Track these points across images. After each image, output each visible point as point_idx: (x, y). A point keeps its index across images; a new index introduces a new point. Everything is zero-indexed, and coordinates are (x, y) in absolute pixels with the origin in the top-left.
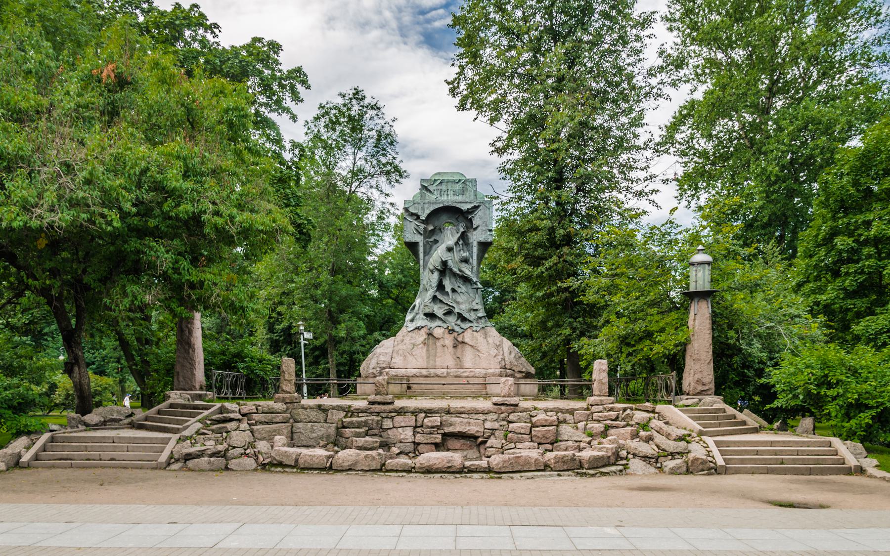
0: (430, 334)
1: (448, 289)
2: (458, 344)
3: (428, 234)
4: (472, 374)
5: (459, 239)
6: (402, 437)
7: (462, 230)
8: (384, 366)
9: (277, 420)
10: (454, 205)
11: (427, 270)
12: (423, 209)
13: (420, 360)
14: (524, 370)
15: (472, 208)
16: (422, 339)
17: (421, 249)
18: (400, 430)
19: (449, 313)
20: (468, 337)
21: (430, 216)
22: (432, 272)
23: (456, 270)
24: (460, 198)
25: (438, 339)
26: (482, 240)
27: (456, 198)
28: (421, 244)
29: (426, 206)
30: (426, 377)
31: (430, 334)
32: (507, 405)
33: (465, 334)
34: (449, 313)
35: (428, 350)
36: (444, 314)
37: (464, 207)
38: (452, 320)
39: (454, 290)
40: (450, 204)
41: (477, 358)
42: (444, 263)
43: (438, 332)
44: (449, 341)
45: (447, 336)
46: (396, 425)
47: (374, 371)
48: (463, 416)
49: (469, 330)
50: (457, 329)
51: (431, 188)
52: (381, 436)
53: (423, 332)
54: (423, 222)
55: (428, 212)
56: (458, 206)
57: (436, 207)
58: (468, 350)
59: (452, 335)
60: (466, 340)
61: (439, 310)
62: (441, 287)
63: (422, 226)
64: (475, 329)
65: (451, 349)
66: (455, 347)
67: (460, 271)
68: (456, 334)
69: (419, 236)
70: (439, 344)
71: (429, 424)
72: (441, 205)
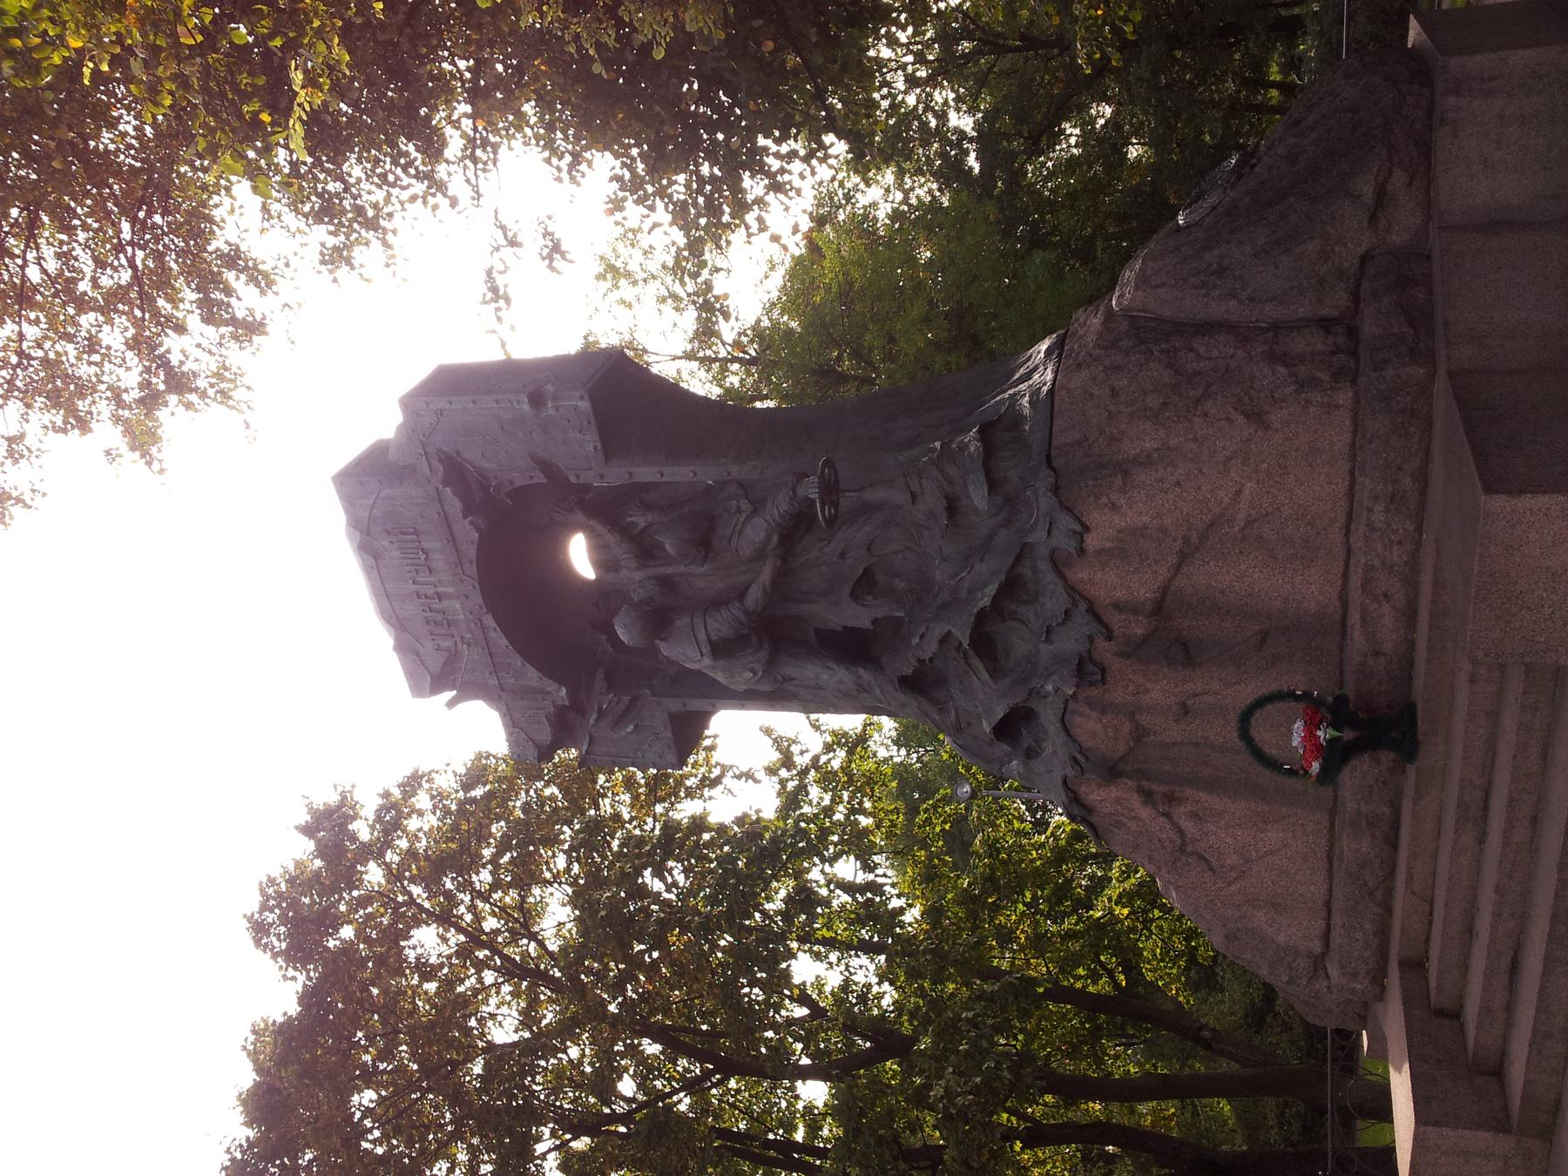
1: (860, 616)
10: (472, 570)
13: (1274, 836)
25: (1139, 734)
26: (590, 442)
28: (675, 705)
35: (1213, 786)
36: (995, 672)
38: (1019, 641)
45: (1118, 696)
49: (1080, 574)
50: (1069, 642)
56: (471, 551)
59: (1115, 664)
60: (1144, 589)
64: (1066, 544)
67: (759, 556)
72: (489, 621)
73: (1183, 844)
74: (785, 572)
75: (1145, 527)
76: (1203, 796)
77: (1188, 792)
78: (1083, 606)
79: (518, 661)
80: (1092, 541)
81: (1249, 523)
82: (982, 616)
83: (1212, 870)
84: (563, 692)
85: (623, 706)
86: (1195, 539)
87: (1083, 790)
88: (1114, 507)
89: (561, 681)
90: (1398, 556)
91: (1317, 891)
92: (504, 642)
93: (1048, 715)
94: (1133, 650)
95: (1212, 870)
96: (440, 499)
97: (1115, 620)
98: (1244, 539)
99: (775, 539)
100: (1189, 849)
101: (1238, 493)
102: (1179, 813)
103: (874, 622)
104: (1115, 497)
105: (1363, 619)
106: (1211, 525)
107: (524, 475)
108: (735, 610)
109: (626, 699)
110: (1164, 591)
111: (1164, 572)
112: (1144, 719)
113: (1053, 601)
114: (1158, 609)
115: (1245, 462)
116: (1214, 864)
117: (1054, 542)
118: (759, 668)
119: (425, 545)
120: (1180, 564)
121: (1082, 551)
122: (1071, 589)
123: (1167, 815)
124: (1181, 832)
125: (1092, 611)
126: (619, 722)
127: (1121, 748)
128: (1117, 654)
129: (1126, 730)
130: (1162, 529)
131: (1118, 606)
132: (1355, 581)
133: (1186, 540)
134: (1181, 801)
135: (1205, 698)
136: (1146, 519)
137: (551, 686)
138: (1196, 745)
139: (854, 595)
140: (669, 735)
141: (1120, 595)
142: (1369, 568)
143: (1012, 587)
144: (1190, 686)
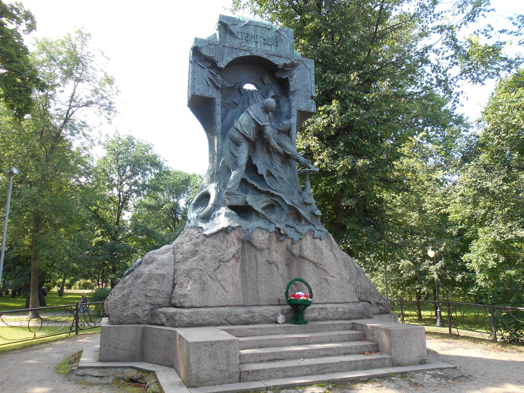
0: (247, 242)
1: (262, 170)
3: (225, 91)
4: (324, 313)
8: (160, 300)
10: (265, 56)
11: (228, 140)
13: (230, 289)
16: (233, 250)
17: (218, 109)
19: (270, 207)
21: (231, 64)
22: (237, 144)
23: (273, 143)
24: (272, 49)
25: (261, 250)
26: (303, 108)
27: (268, 48)
28: (218, 101)
29: (227, 50)
30: (247, 323)
31: (247, 242)
33: (304, 242)
34: (270, 207)
36: (264, 209)
37: (279, 62)
39: (269, 174)
41: (324, 284)
42: (260, 130)
43: (260, 238)
44: (278, 255)
45: (274, 245)
47: (139, 311)
50: (291, 233)
51: (232, 28)
53: (233, 237)
55: (230, 59)
56: (271, 59)
57: (241, 54)
59: (284, 244)
60: (308, 253)
61: (258, 204)
62: (251, 167)
63: (219, 77)
66: (288, 264)
69: (215, 90)
70: (261, 259)
72: (248, 54)
73: (223, 262)
75: (323, 254)
76: (238, 268)
77: (239, 263)
78: (301, 237)
79: (234, 57)
80: (317, 241)
81: (326, 280)
83: (215, 270)
84: (222, 66)
85: (217, 84)
86: (320, 267)
88: (327, 247)
90: (331, 315)
94: (289, 251)
95: (215, 270)
97: (297, 246)
98: (321, 279)
99: (289, 153)
100: (221, 263)
101: (333, 277)
103: (262, 176)
104: (328, 247)
105: (313, 309)
106: (325, 270)
109: (220, 86)
110: (307, 259)
111: (312, 259)
112: (266, 252)
114: (302, 257)
115: (341, 278)
116: (218, 271)
117: (316, 231)
119: (273, 46)
120: (314, 263)
121: (314, 238)
123: (234, 256)
124: (229, 261)
125: (300, 239)
127: (257, 244)
128: (287, 245)
129: (263, 246)
130: (323, 259)
131: (301, 247)
132: (321, 306)
133: (321, 265)
134: (237, 261)
135: (276, 269)
136: (325, 255)
138: (257, 266)
140: (207, 96)
141: (304, 247)
142: (326, 309)
144: (280, 265)
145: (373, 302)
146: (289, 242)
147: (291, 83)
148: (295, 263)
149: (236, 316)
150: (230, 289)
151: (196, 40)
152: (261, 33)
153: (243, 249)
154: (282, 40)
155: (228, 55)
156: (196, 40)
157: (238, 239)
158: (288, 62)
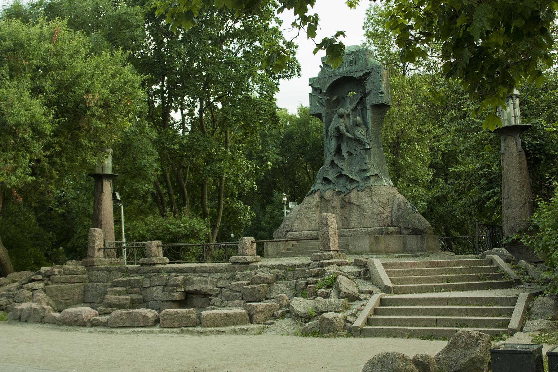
1: (344, 153)
2: (346, 205)
5: (357, 105)
6: (155, 295)
7: (360, 96)
8: (288, 229)
9: (73, 280)
10: (349, 75)
12: (324, 84)
13: (313, 222)
14: (410, 226)
15: (364, 75)
18: (154, 288)
20: (353, 197)
21: (330, 88)
24: (353, 68)
25: (329, 201)
26: (374, 103)
27: (350, 68)
28: (323, 115)
29: (326, 80)
31: (322, 197)
32: (241, 263)
33: (351, 194)
34: (340, 176)
36: (337, 177)
38: (342, 181)
40: (345, 75)
43: (328, 194)
44: (336, 203)
46: (153, 284)
48: (204, 275)
50: (344, 190)
52: (141, 294)
54: (326, 94)
55: (328, 85)
58: (355, 209)
59: (340, 197)
60: (353, 200)
61: (331, 176)
64: (360, 188)
65: (339, 209)
66: (343, 207)
67: (354, 135)
68: (343, 195)
71: (172, 283)
72: (338, 77)
74: (351, 139)
80: (360, 192)
82: (347, 176)
84: (325, 91)
87: (318, 192)
89: (327, 91)
91: (305, 229)
92: (334, 80)
93: (330, 186)
94: (343, 199)
96: (363, 71)
97: (348, 196)
102: (315, 208)
107: (368, 87)
108: (345, 131)
110: (353, 203)
112: (331, 202)
113: (349, 187)
114: (350, 203)
118: (334, 134)
122: (352, 189)
126: (319, 102)
127: (326, 198)
137: (326, 88)
139: (348, 152)
143: (352, 181)
145: (402, 227)
146: (343, 195)
147: (366, 87)
148: (347, 207)
149: (311, 234)
150: (313, 222)
151: (310, 79)
152: (346, 59)
153: (321, 201)
154: (359, 58)
155: (328, 82)
156: (310, 79)
157: (319, 196)
158: (361, 74)
